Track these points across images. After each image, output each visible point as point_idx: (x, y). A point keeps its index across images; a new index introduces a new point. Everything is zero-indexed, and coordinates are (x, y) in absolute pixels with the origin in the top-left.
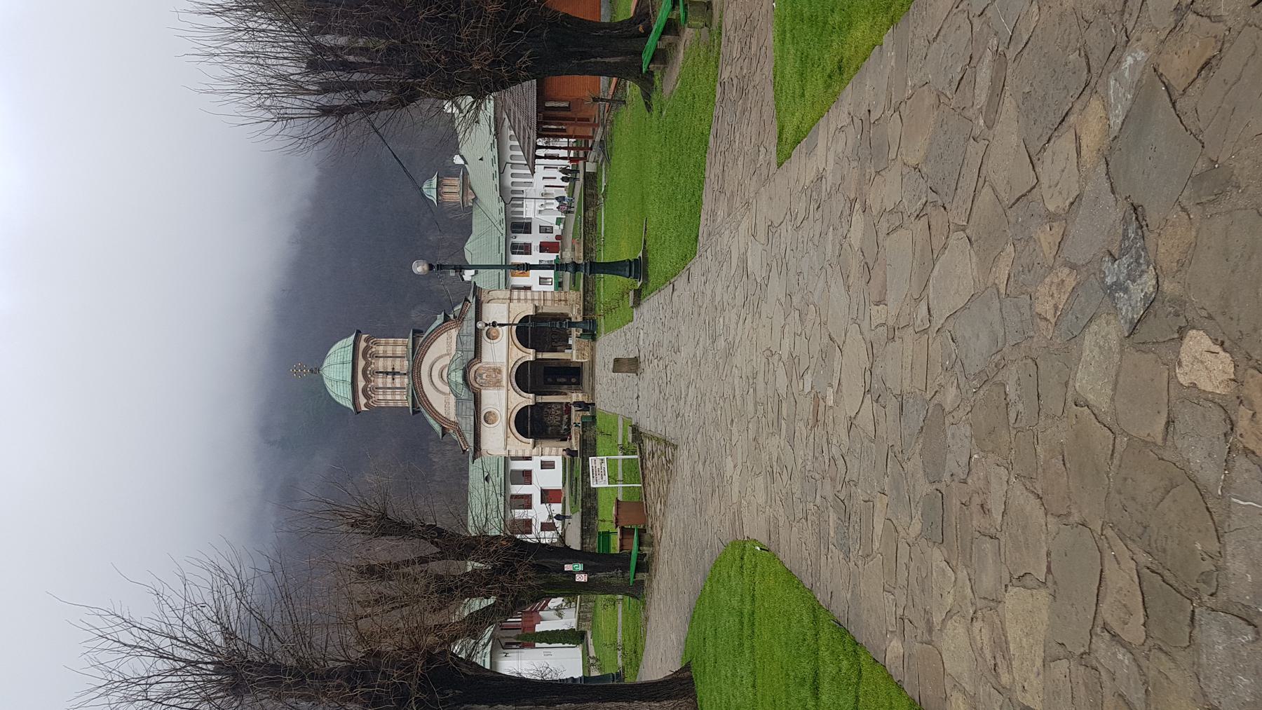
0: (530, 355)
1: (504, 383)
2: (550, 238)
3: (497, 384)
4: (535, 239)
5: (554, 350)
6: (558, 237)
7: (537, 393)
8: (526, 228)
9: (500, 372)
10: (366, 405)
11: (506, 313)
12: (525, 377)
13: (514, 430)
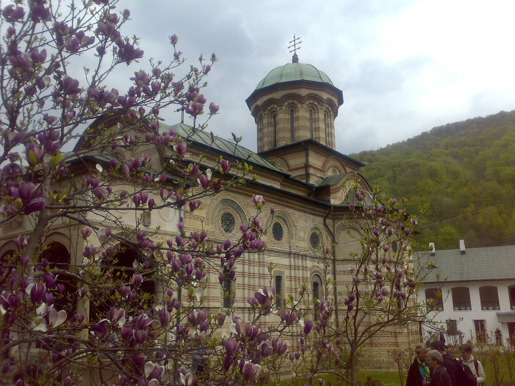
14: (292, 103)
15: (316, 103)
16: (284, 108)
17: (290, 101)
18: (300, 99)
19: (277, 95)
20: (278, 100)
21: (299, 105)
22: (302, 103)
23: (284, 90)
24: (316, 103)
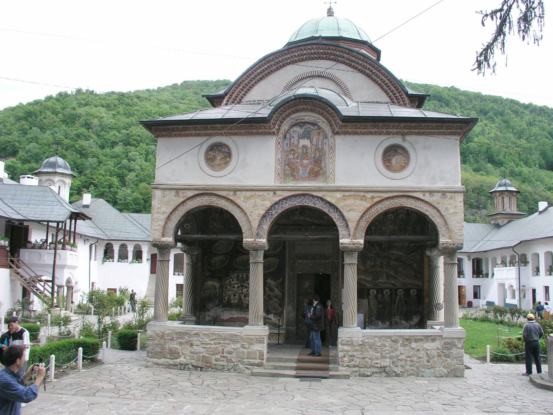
0: (351, 238)
1: (291, 184)
2: (469, 296)
3: (289, 169)
4: (468, 281)
5: (362, 293)
6: (470, 304)
8: (478, 271)
11: (440, 185)
12: (303, 225)
13: (192, 205)
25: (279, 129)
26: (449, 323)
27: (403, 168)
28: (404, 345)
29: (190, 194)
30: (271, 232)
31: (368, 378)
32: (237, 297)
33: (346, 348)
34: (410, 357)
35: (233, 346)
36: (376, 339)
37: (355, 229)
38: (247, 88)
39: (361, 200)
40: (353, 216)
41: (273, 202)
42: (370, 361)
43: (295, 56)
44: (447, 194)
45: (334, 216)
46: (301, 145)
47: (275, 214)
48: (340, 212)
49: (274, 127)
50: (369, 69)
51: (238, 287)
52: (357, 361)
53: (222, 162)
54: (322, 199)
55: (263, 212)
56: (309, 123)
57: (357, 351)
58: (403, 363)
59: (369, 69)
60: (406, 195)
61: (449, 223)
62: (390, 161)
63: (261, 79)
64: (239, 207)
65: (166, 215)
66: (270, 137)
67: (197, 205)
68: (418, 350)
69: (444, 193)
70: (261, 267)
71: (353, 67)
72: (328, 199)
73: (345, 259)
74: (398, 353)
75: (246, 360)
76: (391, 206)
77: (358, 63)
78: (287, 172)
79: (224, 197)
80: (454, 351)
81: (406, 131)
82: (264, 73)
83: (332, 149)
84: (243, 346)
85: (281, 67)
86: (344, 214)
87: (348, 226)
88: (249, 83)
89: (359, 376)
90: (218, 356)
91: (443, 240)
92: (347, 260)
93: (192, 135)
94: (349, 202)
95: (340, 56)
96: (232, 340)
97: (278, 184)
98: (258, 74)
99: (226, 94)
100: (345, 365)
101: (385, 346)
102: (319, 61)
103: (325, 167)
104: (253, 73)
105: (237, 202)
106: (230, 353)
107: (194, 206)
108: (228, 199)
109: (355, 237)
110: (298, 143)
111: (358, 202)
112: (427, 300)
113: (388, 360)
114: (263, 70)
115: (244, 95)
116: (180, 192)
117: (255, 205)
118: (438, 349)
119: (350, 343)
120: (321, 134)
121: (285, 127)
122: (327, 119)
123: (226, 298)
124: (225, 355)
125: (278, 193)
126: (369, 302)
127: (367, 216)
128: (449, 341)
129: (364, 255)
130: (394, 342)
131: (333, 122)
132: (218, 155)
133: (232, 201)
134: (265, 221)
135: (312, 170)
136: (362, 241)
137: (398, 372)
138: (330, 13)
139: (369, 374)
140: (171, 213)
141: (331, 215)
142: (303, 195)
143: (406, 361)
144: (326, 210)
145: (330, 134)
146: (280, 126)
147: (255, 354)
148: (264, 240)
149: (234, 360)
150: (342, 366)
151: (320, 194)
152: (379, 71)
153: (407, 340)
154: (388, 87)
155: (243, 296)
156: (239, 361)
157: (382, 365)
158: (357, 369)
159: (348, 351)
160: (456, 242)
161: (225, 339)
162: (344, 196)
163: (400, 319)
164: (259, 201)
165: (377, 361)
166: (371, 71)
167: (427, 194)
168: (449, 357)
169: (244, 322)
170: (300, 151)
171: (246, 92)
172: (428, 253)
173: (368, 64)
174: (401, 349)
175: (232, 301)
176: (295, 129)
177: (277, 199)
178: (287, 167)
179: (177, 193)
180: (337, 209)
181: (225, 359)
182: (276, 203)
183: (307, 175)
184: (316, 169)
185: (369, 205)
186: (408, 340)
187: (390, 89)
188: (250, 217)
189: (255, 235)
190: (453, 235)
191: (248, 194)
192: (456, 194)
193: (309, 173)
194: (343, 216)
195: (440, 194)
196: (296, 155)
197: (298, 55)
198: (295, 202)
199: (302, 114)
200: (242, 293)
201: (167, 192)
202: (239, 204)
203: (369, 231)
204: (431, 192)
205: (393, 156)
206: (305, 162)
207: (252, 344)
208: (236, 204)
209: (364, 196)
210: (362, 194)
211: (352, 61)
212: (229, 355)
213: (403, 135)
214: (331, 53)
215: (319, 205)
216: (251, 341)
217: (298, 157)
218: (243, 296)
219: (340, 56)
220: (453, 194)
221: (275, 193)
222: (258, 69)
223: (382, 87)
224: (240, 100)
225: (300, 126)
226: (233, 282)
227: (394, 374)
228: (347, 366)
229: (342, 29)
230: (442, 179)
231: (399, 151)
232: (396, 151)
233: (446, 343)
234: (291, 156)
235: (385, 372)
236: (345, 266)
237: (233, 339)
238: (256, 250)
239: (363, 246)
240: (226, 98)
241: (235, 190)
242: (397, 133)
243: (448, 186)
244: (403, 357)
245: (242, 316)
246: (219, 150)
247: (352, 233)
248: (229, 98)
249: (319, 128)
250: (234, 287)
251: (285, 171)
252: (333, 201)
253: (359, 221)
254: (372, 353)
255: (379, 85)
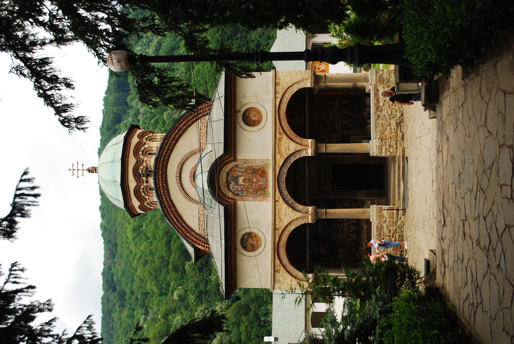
1: (270, 190)
3: (260, 191)
7: (319, 203)
9: (263, 173)
10: (140, 207)
12: (298, 181)
13: (285, 261)
14: (143, 152)
15: (147, 137)
16: (145, 159)
17: (140, 153)
18: (139, 145)
19: (132, 161)
20: (137, 161)
21: (146, 146)
22: (145, 144)
23: (129, 156)
24: (147, 137)
25: (232, 199)
26: (366, 80)
27: (259, 112)
28: (381, 111)
29: (278, 262)
30: (304, 204)
31: (404, 134)
32: (351, 235)
33: (384, 150)
34: (389, 107)
35: (385, 229)
36: (377, 130)
37: (302, 145)
38: (188, 230)
39: (281, 141)
40: (293, 147)
41: (283, 202)
42: (393, 134)
43: (164, 192)
44: (277, 82)
45: (293, 160)
46: (243, 184)
47: (291, 201)
48: (290, 155)
49: (230, 202)
50: (175, 136)
51: (343, 234)
52: (393, 143)
53: (255, 239)
54: (281, 168)
55: (290, 209)
56: (227, 178)
57: (385, 143)
58: (393, 111)
59: (175, 136)
60: (277, 111)
61: (296, 81)
62: (254, 121)
63: (182, 219)
64: (287, 226)
65: (293, 279)
66: (237, 205)
67: (286, 257)
68: (385, 101)
69: (276, 84)
70: (329, 211)
71: (173, 148)
72: (281, 164)
73: (322, 152)
74: (387, 115)
75: (395, 220)
76: (286, 121)
77: (170, 144)
78: (262, 193)
79: (280, 237)
80: (385, 76)
81: (233, 110)
82: (177, 216)
83: (246, 161)
84: (385, 222)
85: (172, 203)
86: (291, 153)
87: (299, 150)
88: (185, 229)
89: (403, 141)
90: (393, 239)
91: (308, 85)
92: (323, 150)
93: (235, 262)
94: (283, 149)
95: (164, 157)
96: (381, 230)
97: (271, 199)
98: (178, 221)
99: (193, 246)
100: (395, 151)
101: (382, 123)
102: (168, 174)
103: (258, 166)
104: (177, 225)
105: (283, 228)
106: (390, 232)
107: (287, 259)
108: (281, 234)
109: (307, 146)
110: (240, 185)
111: (283, 143)
112: (351, 92)
113: (392, 121)
114: (175, 217)
115: (194, 232)
116: (276, 269)
117: (285, 215)
118: (383, 87)
119: (380, 148)
120: (235, 169)
121: (230, 194)
122: (225, 165)
123: (352, 243)
124: (391, 234)
125: (277, 199)
126: (353, 135)
127: (293, 137)
128: (378, 79)
129: (320, 139)
130: (379, 117)
131: (227, 161)
132: (250, 242)
133: (283, 232)
134: (296, 208)
135: (260, 176)
136: (310, 140)
137: (400, 114)
138: (93, 170)
139: (401, 134)
140: (292, 275)
141: (292, 161)
142: (278, 182)
143: (392, 109)
144: (289, 165)
145: (234, 163)
146: (229, 198)
147: (390, 213)
148: (310, 208)
149: (395, 228)
150: (396, 153)
151: (278, 170)
152: (177, 128)
153: (377, 109)
154: (189, 121)
155: (350, 231)
156: (395, 225)
157: (395, 125)
158: (398, 143)
159: (386, 149)
160: (310, 75)
161: (380, 234)
162: (279, 153)
163: (365, 111)
164: (283, 212)
165: (393, 129)
166: (177, 134)
167: (277, 96)
168: (389, 80)
169: (368, 222)
170: (247, 184)
171: (192, 230)
172: (316, 92)
173: (171, 136)
174: (384, 112)
175: (354, 239)
176: (231, 188)
177: (281, 199)
178: (258, 193)
179: (277, 271)
180: (288, 157)
181: (394, 235)
182: (284, 199)
183: (264, 179)
184: (260, 173)
185: (285, 136)
186: (377, 108)
187: (191, 119)
188: (294, 218)
189: (306, 215)
190: (305, 78)
191: (277, 219)
192: (277, 76)
193: (263, 177)
194: (293, 153)
195: (277, 87)
196: (250, 187)
197: (163, 190)
198: (283, 186)
199: (221, 183)
200: (348, 231)
201: (276, 278)
202: (285, 226)
203: (302, 135)
204: (276, 93)
205: (251, 119)
206: (255, 180)
207: (383, 216)
208: (285, 229)
209: (279, 139)
210: (277, 141)
211: (168, 148)
212: (392, 232)
213: (236, 112)
214: (162, 164)
215: (285, 170)
216: (381, 216)
217: (252, 186)
218: (350, 231)
219: (164, 157)
220: (277, 78)
221: (277, 201)
222: (174, 221)
223: (189, 126)
224: (198, 235)
225: (229, 184)
226: (340, 238)
227: (401, 117)
228: (396, 149)
229: (112, 159)
230: (267, 85)
231: (247, 115)
232: (247, 117)
233: (380, 82)
234: (251, 190)
235: (399, 124)
236: (327, 152)
237: (380, 229)
238: (316, 214)
239: (313, 140)
240: (196, 245)
241: (275, 229)
242: (235, 116)
243: (271, 81)
244: (389, 111)
245: (365, 231)
246: (246, 242)
247: (304, 148)
248: (197, 243)
249: (230, 170)
250: (343, 237)
251: (261, 194)
252: (282, 161)
253: (296, 143)
254: (387, 133)
255: (187, 128)
